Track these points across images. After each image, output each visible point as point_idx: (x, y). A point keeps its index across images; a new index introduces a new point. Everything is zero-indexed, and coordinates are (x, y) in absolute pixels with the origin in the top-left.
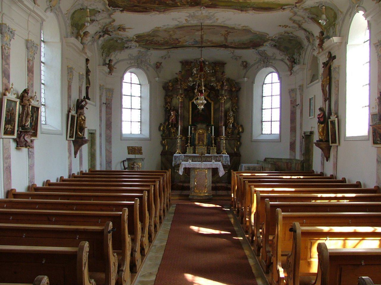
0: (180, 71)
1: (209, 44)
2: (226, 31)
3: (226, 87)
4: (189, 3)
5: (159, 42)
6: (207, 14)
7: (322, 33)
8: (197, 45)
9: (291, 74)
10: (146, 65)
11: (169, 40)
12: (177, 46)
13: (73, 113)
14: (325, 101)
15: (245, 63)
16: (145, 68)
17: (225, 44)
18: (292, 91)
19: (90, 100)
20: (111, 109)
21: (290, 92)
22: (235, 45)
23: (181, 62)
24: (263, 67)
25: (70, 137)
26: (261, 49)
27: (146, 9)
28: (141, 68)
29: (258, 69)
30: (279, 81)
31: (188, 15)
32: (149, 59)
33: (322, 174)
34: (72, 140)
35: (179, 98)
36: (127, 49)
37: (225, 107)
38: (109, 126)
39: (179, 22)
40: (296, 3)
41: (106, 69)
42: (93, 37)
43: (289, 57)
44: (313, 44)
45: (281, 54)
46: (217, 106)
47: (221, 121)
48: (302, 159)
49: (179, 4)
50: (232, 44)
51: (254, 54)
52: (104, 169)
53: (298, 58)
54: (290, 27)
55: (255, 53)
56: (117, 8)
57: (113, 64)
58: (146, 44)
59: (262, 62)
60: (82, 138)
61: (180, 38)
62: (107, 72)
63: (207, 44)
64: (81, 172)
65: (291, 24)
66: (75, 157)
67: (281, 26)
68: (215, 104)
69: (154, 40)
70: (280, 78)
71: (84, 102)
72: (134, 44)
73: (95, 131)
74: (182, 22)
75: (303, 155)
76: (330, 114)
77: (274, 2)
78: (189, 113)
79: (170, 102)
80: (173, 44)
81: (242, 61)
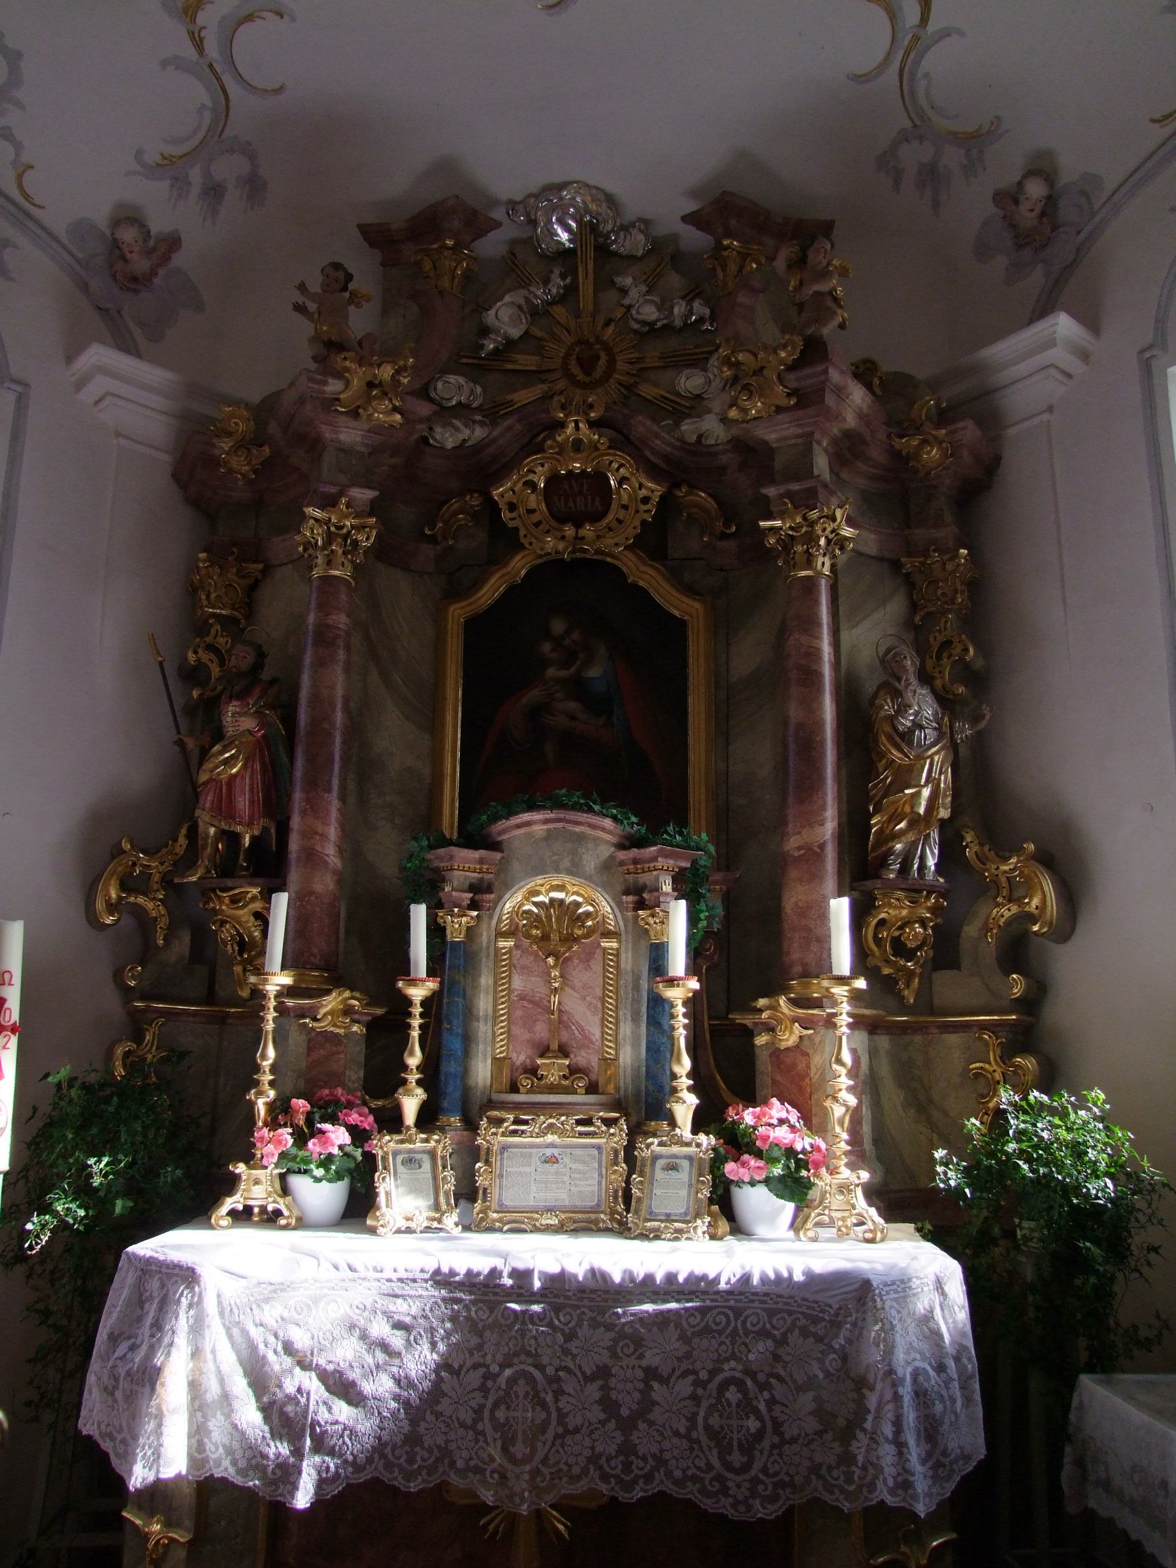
15: (1036, 190)
37: (845, 636)
47: (810, 784)
78: (433, 726)
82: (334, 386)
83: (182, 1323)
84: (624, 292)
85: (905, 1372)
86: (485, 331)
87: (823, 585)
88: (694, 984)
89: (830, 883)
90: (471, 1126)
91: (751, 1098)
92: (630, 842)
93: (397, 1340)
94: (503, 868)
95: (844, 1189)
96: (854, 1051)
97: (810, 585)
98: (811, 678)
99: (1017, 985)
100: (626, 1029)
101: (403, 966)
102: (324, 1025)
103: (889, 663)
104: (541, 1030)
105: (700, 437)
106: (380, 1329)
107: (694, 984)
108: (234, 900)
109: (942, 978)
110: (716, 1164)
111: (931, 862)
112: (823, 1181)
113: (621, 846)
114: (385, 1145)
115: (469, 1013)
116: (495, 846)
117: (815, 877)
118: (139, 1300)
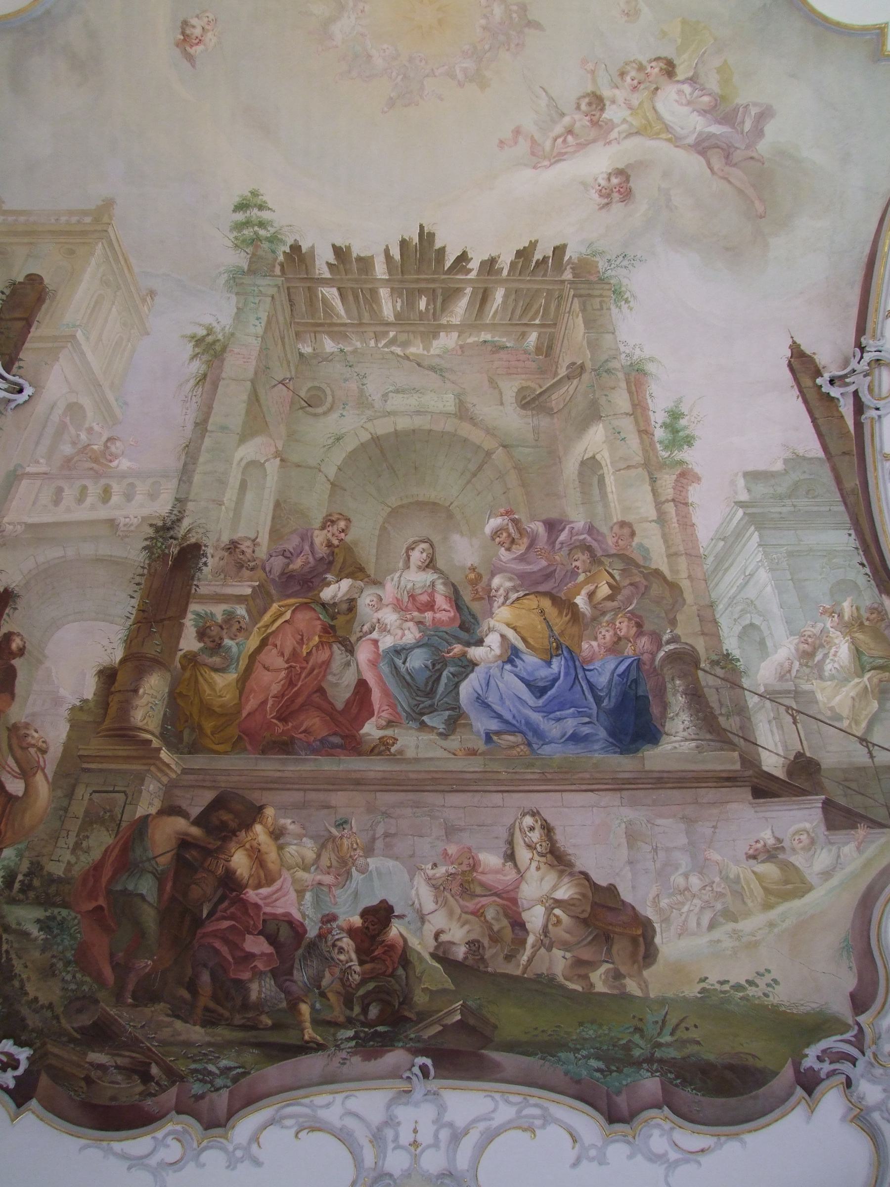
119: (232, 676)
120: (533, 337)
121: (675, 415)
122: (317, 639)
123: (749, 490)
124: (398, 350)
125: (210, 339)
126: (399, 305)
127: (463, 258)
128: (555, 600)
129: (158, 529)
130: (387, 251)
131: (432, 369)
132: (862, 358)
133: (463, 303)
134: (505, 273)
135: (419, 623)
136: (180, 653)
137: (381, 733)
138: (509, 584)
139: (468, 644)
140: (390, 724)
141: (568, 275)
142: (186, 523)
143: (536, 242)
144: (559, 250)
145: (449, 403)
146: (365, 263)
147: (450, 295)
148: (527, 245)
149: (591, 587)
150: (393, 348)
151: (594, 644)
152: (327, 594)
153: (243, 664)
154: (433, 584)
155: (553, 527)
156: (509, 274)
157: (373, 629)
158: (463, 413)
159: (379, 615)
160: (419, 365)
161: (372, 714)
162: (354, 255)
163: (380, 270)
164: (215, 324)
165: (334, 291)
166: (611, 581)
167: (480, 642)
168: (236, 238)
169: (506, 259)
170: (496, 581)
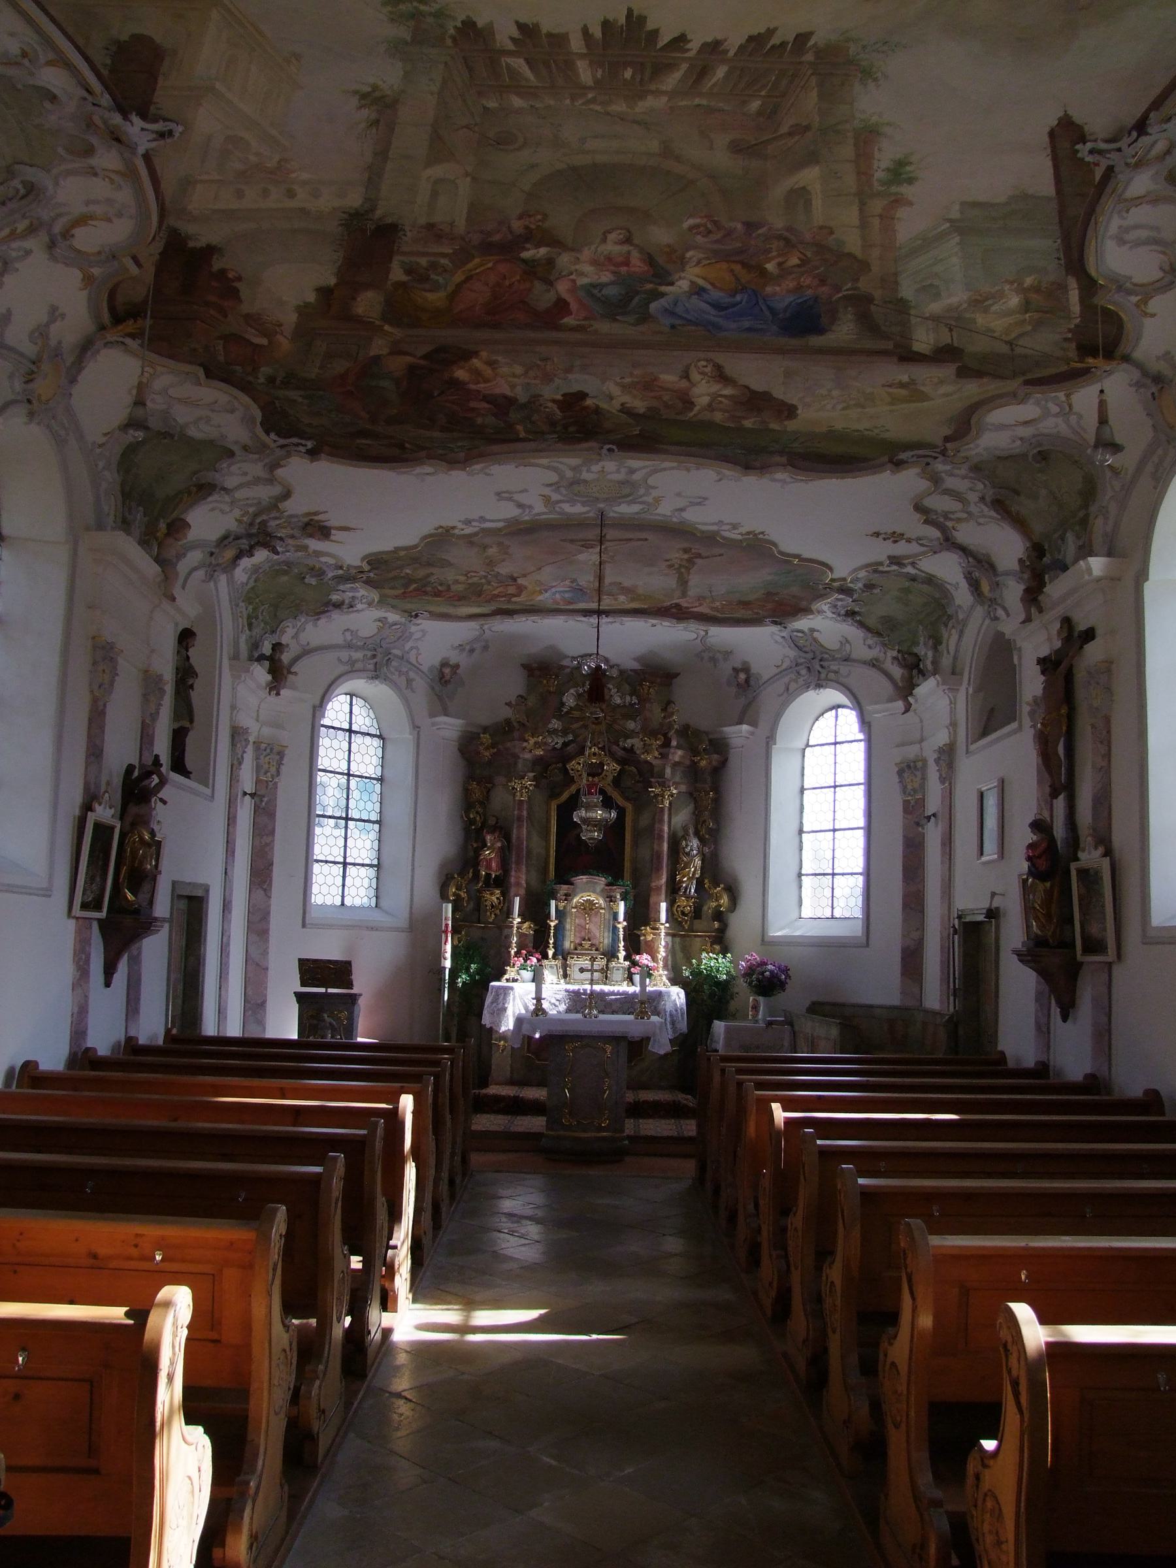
0: (521, 697)
1: (623, 601)
2: (686, 551)
3: (677, 755)
4: (558, 429)
5: (449, 588)
6: (620, 477)
7: (1037, 550)
8: (582, 606)
9: (907, 710)
10: (404, 670)
11: (483, 581)
12: (510, 607)
13: (104, 813)
14: (1054, 794)
15: (742, 676)
16: (402, 681)
17: (677, 601)
18: (910, 769)
19: (189, 778)
20: (272, 815)
21: (900, 773)
22: (712, 608)
23: (525, 666)
24: (807, 687)
25: (85, 906)
26: (803, 623)
27: (402, 447)
28: (386, 679)
29: (789, 695)
30: (861, 736)
31: (553, 477)
32: (414, 652)
33: (1042, 1070)
34: (99, 920)
35: (513, 788)
36: (337, 611)
37: (673, 821)
38: (261, 875)
39: (520, 506)
40: (947, 439)
41: (261, 673)
42: (212, 554)
43: (899, 651)
44: (993, 601)
45: (870, 642)
46: (644, 820)
47: (658, 869)
48: (952, 1009)
49: (520, 428)
50: (701, 605)
51: (776, 642)
52: (234, 1029)
53: (930, 654)
54: (909, 541)
55: (781, 640)
56: (295, 440)
57: (286, 658)
58: (404, 596)
59: (804, 672)
60: (137, 912)
61: (524, 576)
62: (264, 685)
63: (616, 599)
64: (130, 1041)
65: (915, 527)
66: (108, 984)
67: (881, 537)
68: (638, 810)
69: (432, 579)
70: (865, 724)
71: (154, 776)
72: (362, 592)
73: (207, 889)
74: (530, 507)
75: (955, 995)
76: (1074, 842)
77: (866, 433)
79: (485, 802)
80: (498, 596)
81: (734, 669)
82: (525, 744)
83: (512, 996)
84: (610, 690)
85: (668, 1010)
86: (563, 704)
87: (666, 809)
88: (625, 923)
89: (663, 896)
90: (565, 959)
91: (639, 953)
92: (608, 885)
93: (557, 1003)
94: (574, 890)
95: (660, 976)
96: (666, 942)
97: (662, 810)
98: (661, 837)
99: (716, 925)
100: (606, 934)
101: (548, 916)
102: (524, 931)
103: (685, 829)
104: (583, 934)
105: (633, 745)
106: (553, 1001)
107: (625, 923)
108: (491, 894)
109: (696, 922)
110: (629, 969)
111: (693, 891)
112: (656, 973)
113: (607, 885)
114: (545, 962)
115: (564, 928)
116: (572, 884)
117: (659, 894)
118: (497, 995)
119: (442, 294)
120: (755, 105)
121: (901, 164)
122: (518, 277)
123: (962, 213)
124: (598, 108)
125: (377, 94)
126: (599, 74)
127: (680, 40)
128: (744, 264)
129: (350, 215)
130: (585, 31)
131: (635, 122)
132: (1136, 141)
133: (677, 75)
134: (731, 54)
135: (614, 273)
136: (389, 283)
137: (578, 323)
138: (702, 256)
139: (660, 284)
140: (585, 319)
141: (809, 57)
142: (379, 213)
143: (776, 29)
144: (802, 39)
145: (654, 145)
146: (559, 40)
147: (660, 69)
148: (762, 31)
149: (780, 260)
150: (592, 106)
151: (778, 289)
152: (526, 255)
153: (450, 289)
154: (629, 252)
155: (750, 226)
156: (735, 54)
157: (572, 274)
158: (667, 151)
159: (577, 267)
160: (622, 119)
161: (571, 314)
162: (544, 31)
163: (577, 44)
164: (380, 83)
165: (521, 61)
166: (801, 256)
167: (672, 284)
168: (391, 13)
169: (734, 42)
170: (689, 254)
